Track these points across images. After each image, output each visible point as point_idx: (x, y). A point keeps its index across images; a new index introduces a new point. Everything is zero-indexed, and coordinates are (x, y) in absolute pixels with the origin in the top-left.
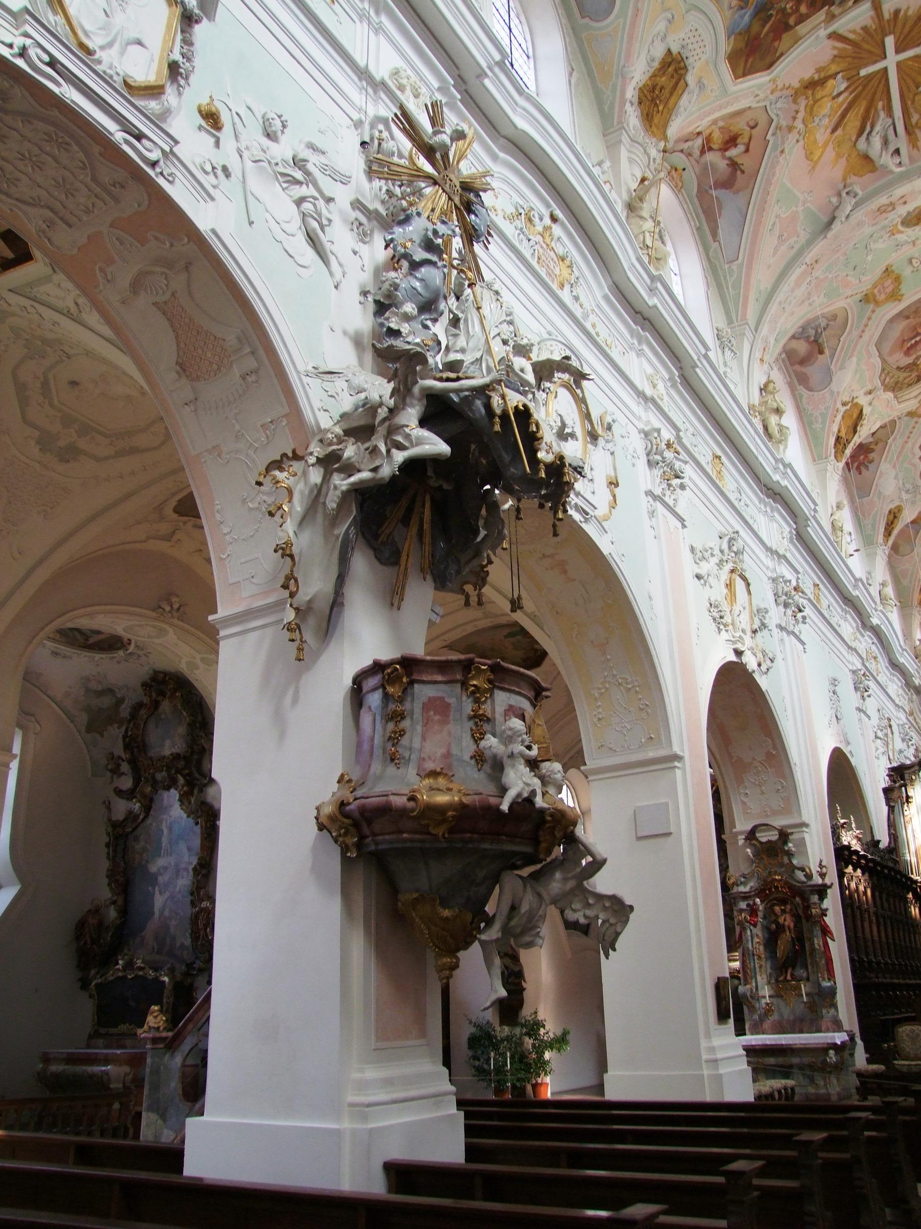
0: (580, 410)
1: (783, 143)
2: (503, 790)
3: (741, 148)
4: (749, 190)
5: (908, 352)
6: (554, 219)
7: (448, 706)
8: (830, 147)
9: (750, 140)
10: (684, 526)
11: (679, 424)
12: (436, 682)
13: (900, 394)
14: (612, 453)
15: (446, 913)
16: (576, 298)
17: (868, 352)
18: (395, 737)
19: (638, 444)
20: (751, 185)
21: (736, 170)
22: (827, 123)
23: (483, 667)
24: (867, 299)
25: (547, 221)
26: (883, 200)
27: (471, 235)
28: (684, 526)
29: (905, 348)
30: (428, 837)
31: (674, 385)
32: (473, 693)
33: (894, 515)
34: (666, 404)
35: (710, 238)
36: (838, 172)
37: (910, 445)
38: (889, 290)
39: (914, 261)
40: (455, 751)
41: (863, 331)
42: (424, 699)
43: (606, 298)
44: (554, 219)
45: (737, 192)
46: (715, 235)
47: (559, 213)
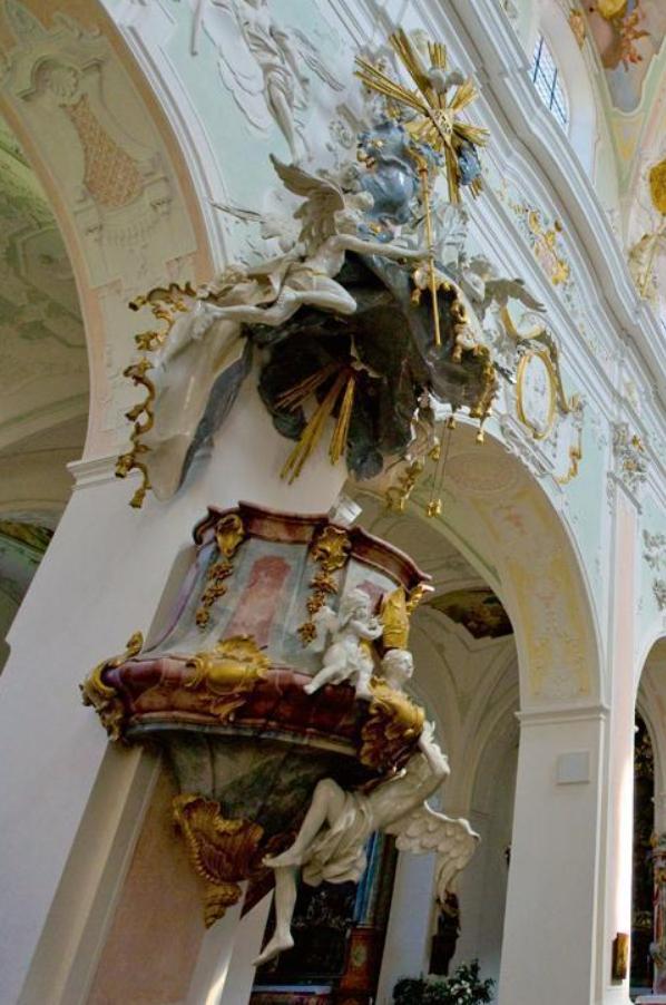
0: (552, 381)
6: (558, 228)
7: (285, 568)
10: (640, 513)
11: (647, 429)
12: (278, 541)
14: (580, 430)
15: (224, 825)
16: (569, 298)
19: (606, 432)
23: (340, 532)
25: (552, 227)
27: (458, 177)
28: (640, 513)
30: (210, 718)
31: (648, 400)
32: (321, 559)
34: (639, 409)
40: (278, 619)
42: (258, 557)
43: (595, 307)
44: (558, 228)
47: (563, 223)
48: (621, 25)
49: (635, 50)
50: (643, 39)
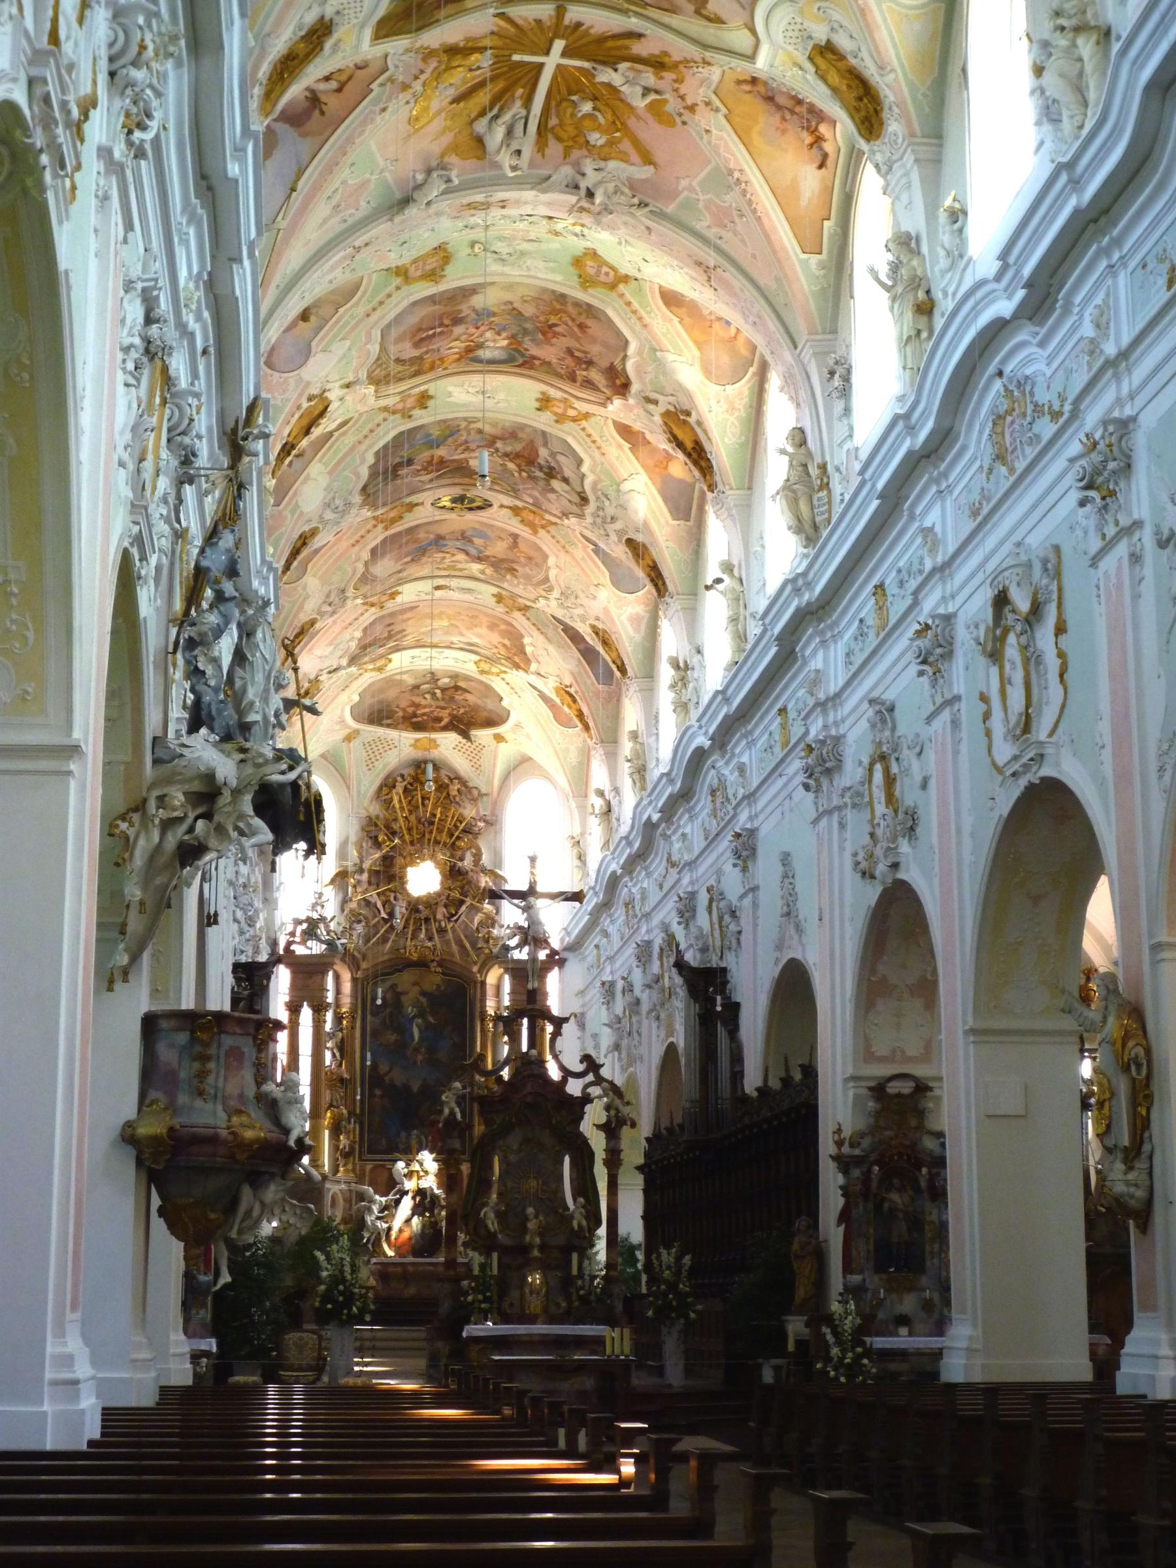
1: (389, 99)
2: (287, 1131)
3: (333, 85)
4: (323, 138)
5: (416, 345)
8: (443, 115)
9: (350, 78)
13: (383, 388)
15: (212, 1216)
17: (369, 334)
18: (202, 1075)
20: (327, 133)
21: (315, 107)
22: (452, 92)
26: (480, 198)
29: (417, 338)
33: (304, 540)
36: (436, 148)
37: (363, 447)
38: (428, 267)
39: (477, 247)
41: (374, 309)
45: (304, 135)
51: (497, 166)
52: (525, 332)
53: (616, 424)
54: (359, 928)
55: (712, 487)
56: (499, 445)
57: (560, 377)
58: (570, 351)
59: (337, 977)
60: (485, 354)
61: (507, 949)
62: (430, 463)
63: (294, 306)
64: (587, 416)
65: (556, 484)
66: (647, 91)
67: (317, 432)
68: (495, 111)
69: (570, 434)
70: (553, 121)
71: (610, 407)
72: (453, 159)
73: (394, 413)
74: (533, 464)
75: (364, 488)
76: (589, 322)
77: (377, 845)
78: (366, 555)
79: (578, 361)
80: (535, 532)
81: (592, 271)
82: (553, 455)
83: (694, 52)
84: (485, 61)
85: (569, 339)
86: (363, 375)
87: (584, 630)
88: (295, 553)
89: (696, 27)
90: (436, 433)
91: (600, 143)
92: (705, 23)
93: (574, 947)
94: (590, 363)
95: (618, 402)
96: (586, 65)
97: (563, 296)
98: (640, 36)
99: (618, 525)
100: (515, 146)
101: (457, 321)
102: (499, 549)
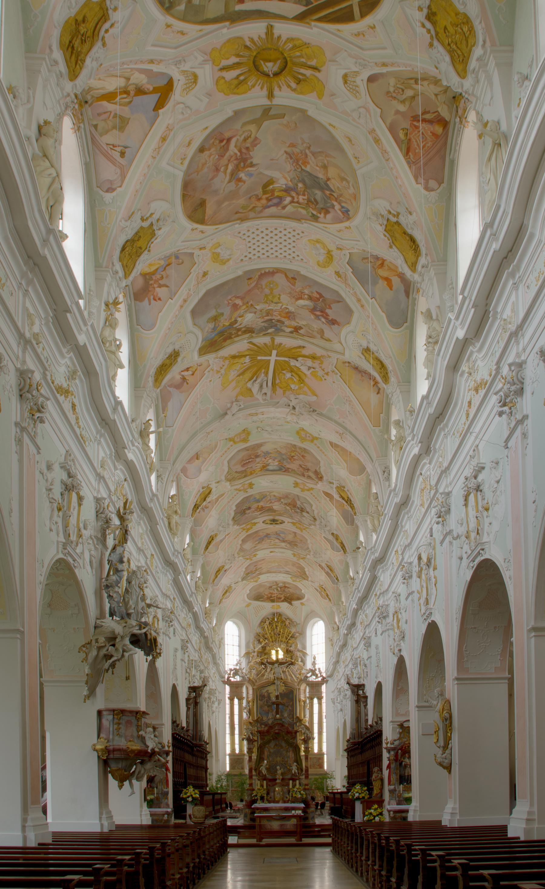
3: (190, 372)
24: (231, 440)
26: (254, 412)
35: (161, 411)
46: (164, 410)
48: (151, 279)
49: (157, 294)
50: (164, 289)
51: (258, 399)
52: (284, 459)
53: (323, 492)
54: (254, 672)
55: (355, 514)
56: (282, 500)
57: (298, 474)
58: (301, 466)
59: (247, 688)
60: (270, 468)
61: (307, 677)
62: (258, 508)
63: (186, 455)
64: (312, 489)
65: (304, 514)
66: (309, 368)
67: (208, 500)
68: (255, 378)
69: (306, 495)
70: (277, 381)
71: (318, 486)
72: (240, 397)
73: (240, 491)
74: (296, 506)
75: (233, 518)
76: (305, 455)
77: (259, 642)
78: (240, 542)
79: (304, 469)
80: (302, 531)
81: (304, 436)
82: (302, 503)
83: (324, 353)
84: (247, 359)
85: (296, 461)
86: (223, 478)
87: (323, 565)
88: (209, 543)
89: (322, 343)
90: (258, 497)
91: (297, 387)
92: (325, 341)
93: (331, 676)
94: (308, 470)
95: (320, 483)
96: (287, 359)
97: (295, 445)
98: (304, 347)
99: (328, 528)
100: (264, 391)
101: (257, 456)
102: (290, 537)
